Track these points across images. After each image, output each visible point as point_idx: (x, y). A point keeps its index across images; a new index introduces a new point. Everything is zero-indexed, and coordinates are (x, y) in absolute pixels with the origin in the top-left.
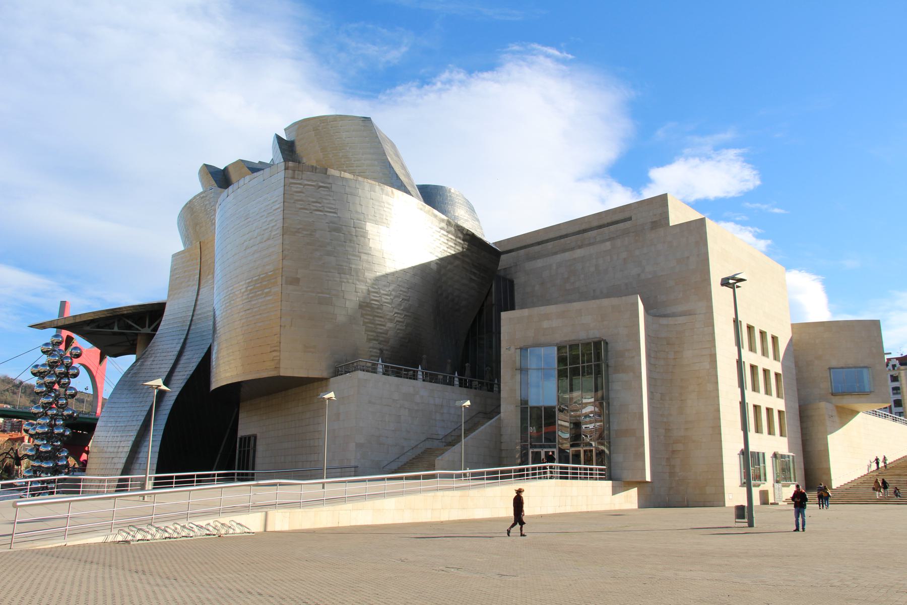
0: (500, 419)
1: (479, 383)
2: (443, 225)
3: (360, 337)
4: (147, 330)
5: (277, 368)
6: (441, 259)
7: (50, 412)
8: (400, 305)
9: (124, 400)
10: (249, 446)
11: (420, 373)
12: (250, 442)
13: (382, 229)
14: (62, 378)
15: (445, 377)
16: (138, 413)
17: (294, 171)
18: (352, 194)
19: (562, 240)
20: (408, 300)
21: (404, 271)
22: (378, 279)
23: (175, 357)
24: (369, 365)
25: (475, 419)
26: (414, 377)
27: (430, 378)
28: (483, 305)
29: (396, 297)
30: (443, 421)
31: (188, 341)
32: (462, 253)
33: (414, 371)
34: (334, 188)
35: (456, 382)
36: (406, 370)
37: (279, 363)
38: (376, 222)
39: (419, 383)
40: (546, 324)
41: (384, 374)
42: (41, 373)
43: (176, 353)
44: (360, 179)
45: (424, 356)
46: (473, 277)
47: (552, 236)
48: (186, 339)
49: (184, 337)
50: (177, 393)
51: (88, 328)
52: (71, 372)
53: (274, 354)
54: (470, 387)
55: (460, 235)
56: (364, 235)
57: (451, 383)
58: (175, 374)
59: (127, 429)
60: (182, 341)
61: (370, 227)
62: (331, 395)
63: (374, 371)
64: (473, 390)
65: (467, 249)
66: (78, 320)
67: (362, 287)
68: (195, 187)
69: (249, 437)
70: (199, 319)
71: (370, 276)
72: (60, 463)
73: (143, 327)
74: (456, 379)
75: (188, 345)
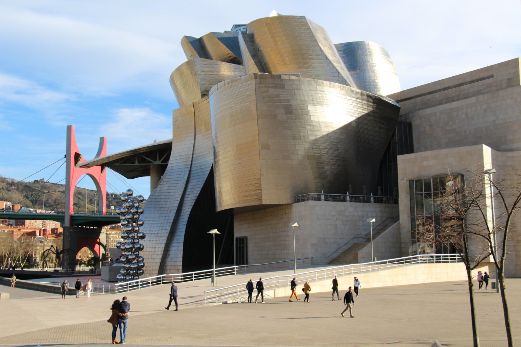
0: (399, 223)
1: (387, 198)
2: (359, 96)
3: (309, 177)
4: (158, 162)
5: (260, 200)
6: (359, 119)
7: (130, 236)
8: (333, 154)
9: (153, 215)
10: (243, 244)
11: (348, 197)
12: (243, 241)
13: (318, 108)
14: (134, 215)
15: (364, 197)
16: (165, 224)
17: (260, 79)
18: (298, 89)
19: (446, 91)
20: (338, 150)
21: (334, 132)
22: (316, 140)
23: (184, 184)
24: (316, 196)
25: (380, 229)
26: (344, 200)
27: (355, 199)
28: (390, 143)
29: (330, 149)
30: (365, 225)
31: (192, 172)
32: (373, 112)
33: (344, 196)
34: (286, 87)
35: (372, 200)
36: (338, 196)
37: (261, 197)
38: (314, 104)
39: (348, 204)
40: (425, 163)
41: (325, 200)
42: (123, 213)
43: (185, 181)
44: (302, 78)
45: (350, 185)
46: (382, 126)
47: (439, 87)
48: (190, 171)
49: (189, 169)
50: (190, 210)
51: (117, 164)
52: (139, 211)
53: (258, 191)
54: (381, 202)
55: (371, 100)
56: (307, 113)
57: (368, 201)
58: (186, 196)
59: (159, 235)
60: (187, 173)
61: (310, 108)
62: (296, 224)
63: (319, 199)
64: (383, 204)
65: (376, 108)
66: (111, 160)
67: (307, 145)
68: (181, 57)
69: (243, 239)
70: (198, 156)
71: (312, 138)
72: (140, 265)
73: (155, 160)
74: (372, 198)
75: (192, 176)
